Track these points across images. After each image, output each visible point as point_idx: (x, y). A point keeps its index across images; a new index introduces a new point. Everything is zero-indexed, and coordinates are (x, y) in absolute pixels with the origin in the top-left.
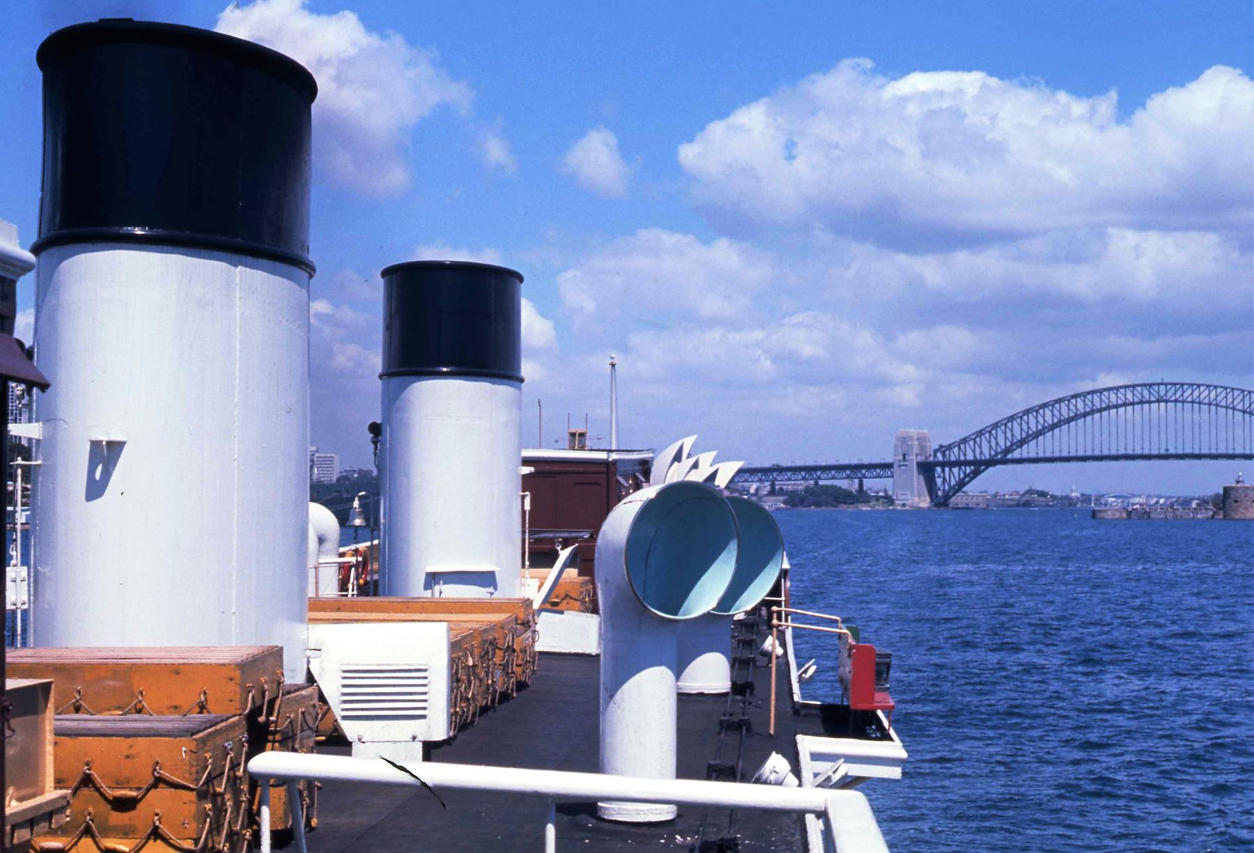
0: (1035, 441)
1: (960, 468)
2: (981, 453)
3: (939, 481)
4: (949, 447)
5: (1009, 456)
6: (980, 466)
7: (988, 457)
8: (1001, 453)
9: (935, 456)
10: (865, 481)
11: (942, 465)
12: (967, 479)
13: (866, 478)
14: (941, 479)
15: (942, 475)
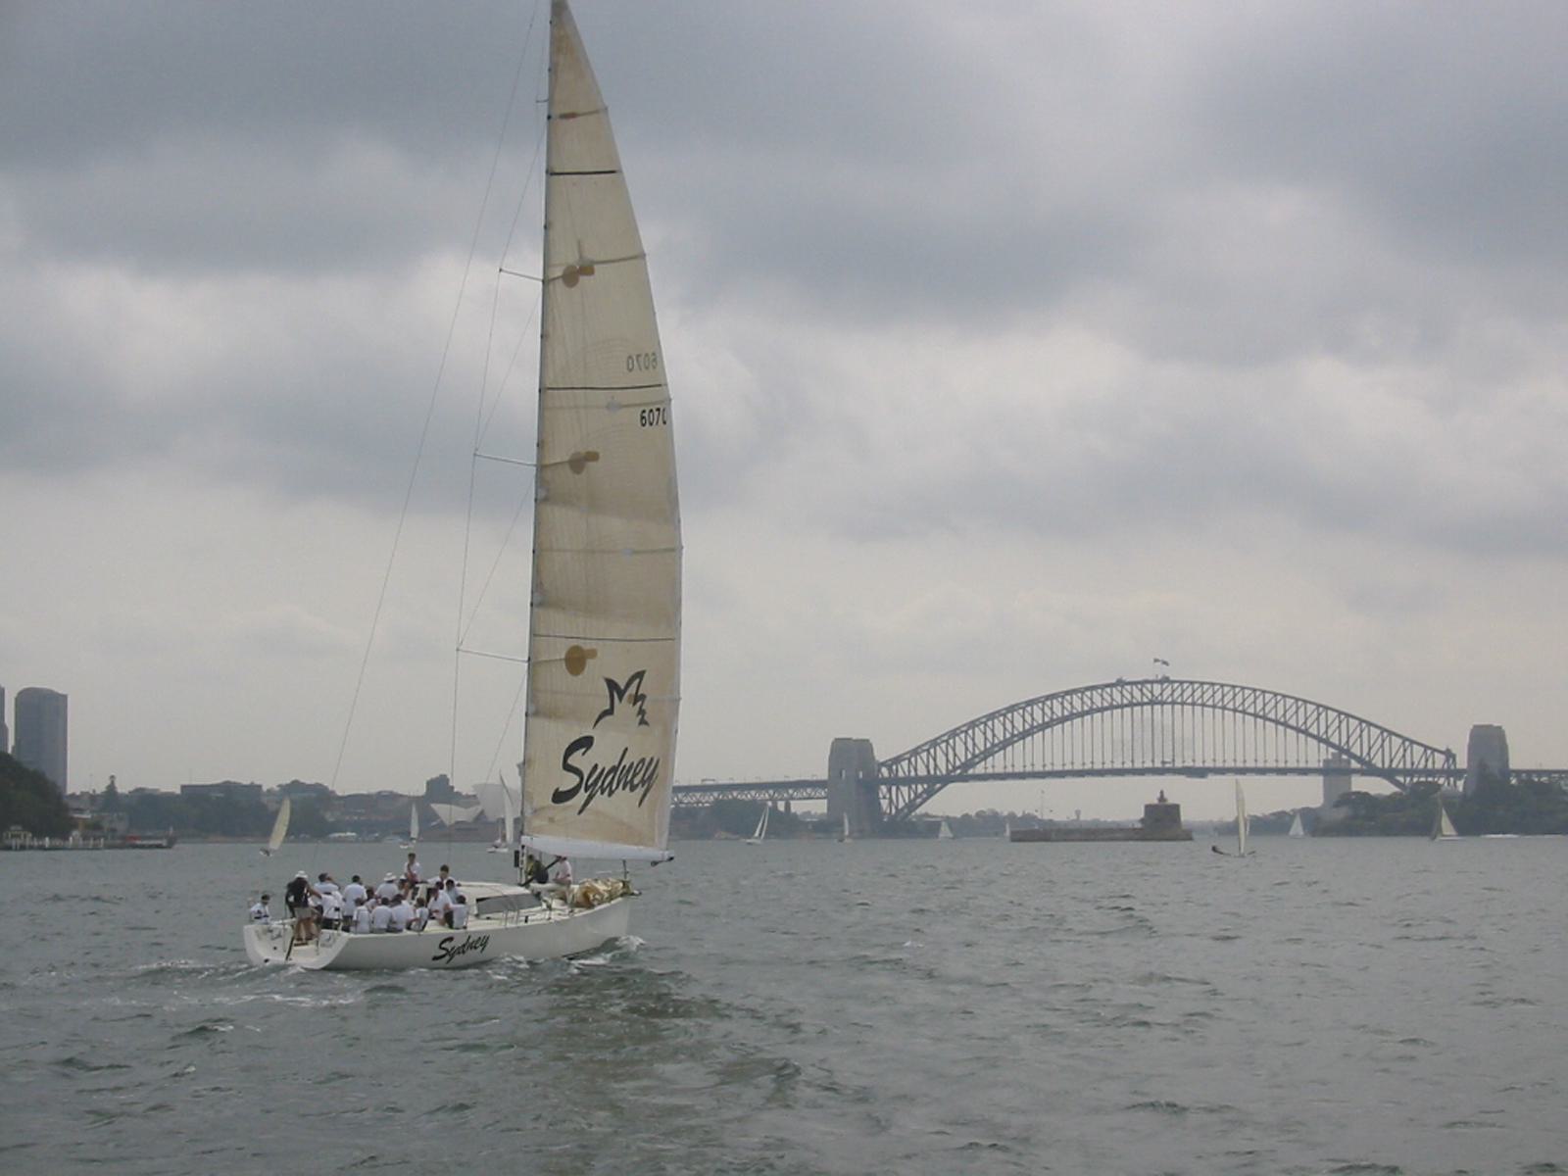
0: (1002, 752)
1: (910, 788)
2: (936, 766)
3: (884, 803)
4: (897, 760)
5: (971, 772)
6: (935, 783)
7: (944, 772)
8: (959, 767)
9: (879, 771)
10: (792, 802)
11: (885, 781)
12: (919, 801)
13: (793, 799)
14: (887, 801)
15: (888, 796)
